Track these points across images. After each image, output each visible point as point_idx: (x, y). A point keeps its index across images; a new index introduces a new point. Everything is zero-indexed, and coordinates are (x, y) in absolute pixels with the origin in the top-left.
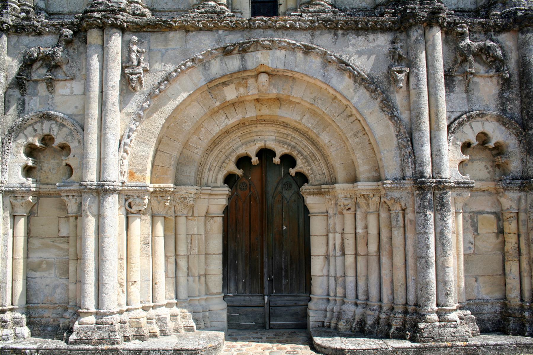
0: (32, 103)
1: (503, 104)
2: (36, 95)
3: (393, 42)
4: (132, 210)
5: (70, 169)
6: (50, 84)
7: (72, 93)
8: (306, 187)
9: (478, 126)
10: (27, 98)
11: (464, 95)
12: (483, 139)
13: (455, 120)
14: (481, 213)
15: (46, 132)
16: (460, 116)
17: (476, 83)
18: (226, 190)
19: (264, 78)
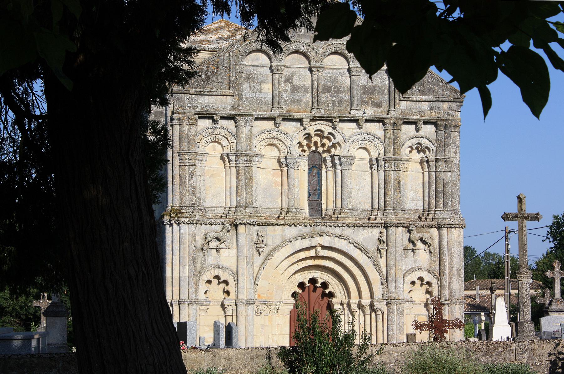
0: (209, 260)
1: (431, 263)
2: (211, 256)
3: (380, 233)
4: (259, 312)
5: (228, 293)
6: (218, 250)
7: (229, 256)
8: (334, 300)
9: (419, 274)
10: (206, 257)
11: (413, 259)
12: (421, 279)
13: (408, 271)
14: (419, 315)
15: (217, 274)
16: (410, 270)
17: (418, 253)
18: (293, 301)
19: (319, 249)
